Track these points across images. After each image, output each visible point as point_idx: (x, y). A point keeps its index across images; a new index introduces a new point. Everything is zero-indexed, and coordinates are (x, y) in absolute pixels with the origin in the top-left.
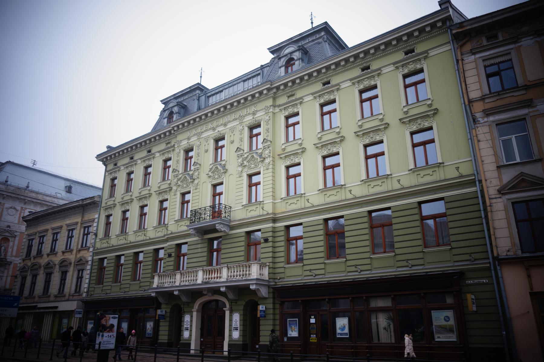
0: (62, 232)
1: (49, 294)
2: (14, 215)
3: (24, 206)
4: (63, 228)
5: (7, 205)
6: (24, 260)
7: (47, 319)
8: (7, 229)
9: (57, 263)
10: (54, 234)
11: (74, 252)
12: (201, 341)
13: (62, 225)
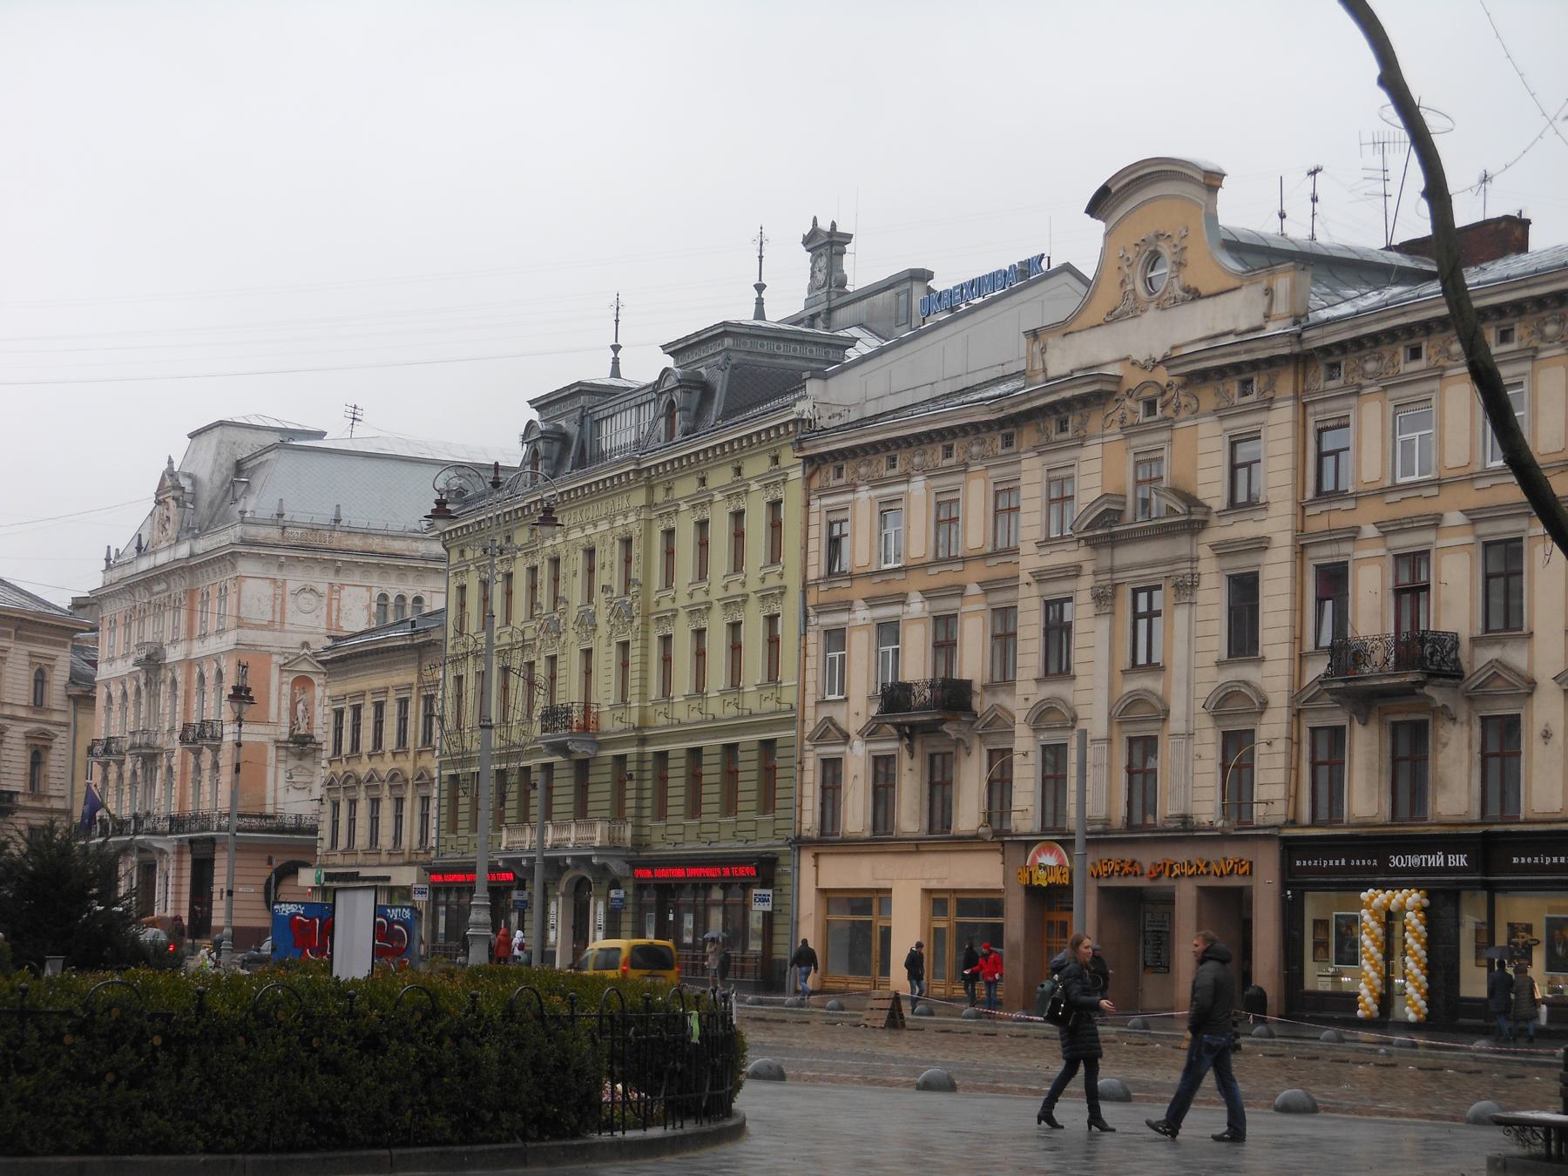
1: (378, 847)
5: (292, 586)
8: (302, 653)
9: (384, 775)
11: (412, 754)
12: (574, 949)
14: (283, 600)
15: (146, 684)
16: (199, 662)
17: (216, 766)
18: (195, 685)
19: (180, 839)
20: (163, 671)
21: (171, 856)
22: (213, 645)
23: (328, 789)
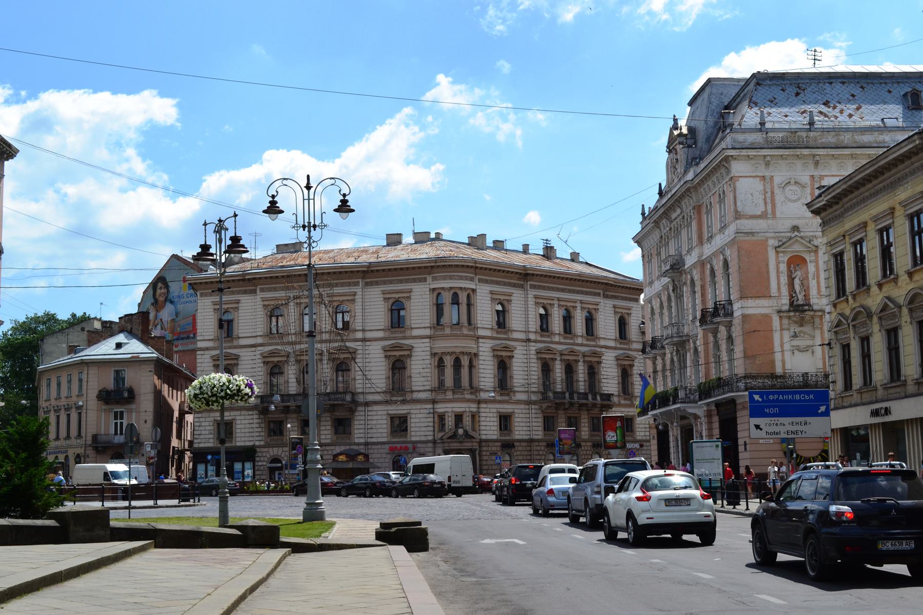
0: (896, 225)
1: (903, 378)
2: (799, 199)
3: (816, 173)
4: (897, 214)
5: (777, 180)
6: (835, 306)
7: (877, 435)
8: (793, 235)
10: (881, 231)
13: (891, 205)
14: (773, 193)
15: (673, 290)
16: (709, 259)
17: (730, 339)
18: (708, 279)
19: (708, 404)
20: (684, 276)
21: (703, 419)
22: (719, 241)
23: (836, 333)
